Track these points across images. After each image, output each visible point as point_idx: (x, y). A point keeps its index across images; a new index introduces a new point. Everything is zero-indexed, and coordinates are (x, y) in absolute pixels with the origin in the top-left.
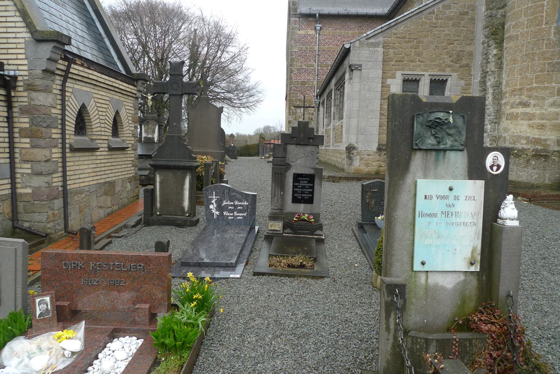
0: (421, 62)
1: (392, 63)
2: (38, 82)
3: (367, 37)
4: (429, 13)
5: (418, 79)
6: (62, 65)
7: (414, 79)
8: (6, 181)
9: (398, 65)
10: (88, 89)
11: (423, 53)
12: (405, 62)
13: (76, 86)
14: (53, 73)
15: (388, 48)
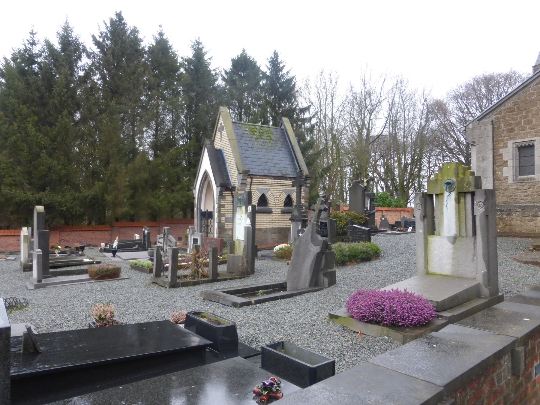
0: (532, 129)
1: (503, 135)
2: (239, 188)
3: (478, 119)
4: (536, 85)
5: (531, 144)
6: (249, 180)
7: (527, 145)
8: (231, 223)
9: (509, 136)
10: (267, 187)
11: (532, 121)
12: (516, 132)
13: (259, 187)
14: (246, 184)
15: (499, 123)
